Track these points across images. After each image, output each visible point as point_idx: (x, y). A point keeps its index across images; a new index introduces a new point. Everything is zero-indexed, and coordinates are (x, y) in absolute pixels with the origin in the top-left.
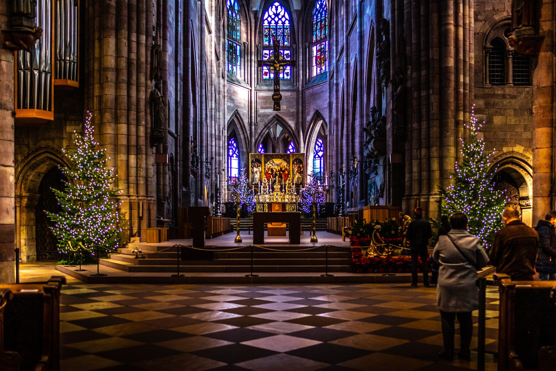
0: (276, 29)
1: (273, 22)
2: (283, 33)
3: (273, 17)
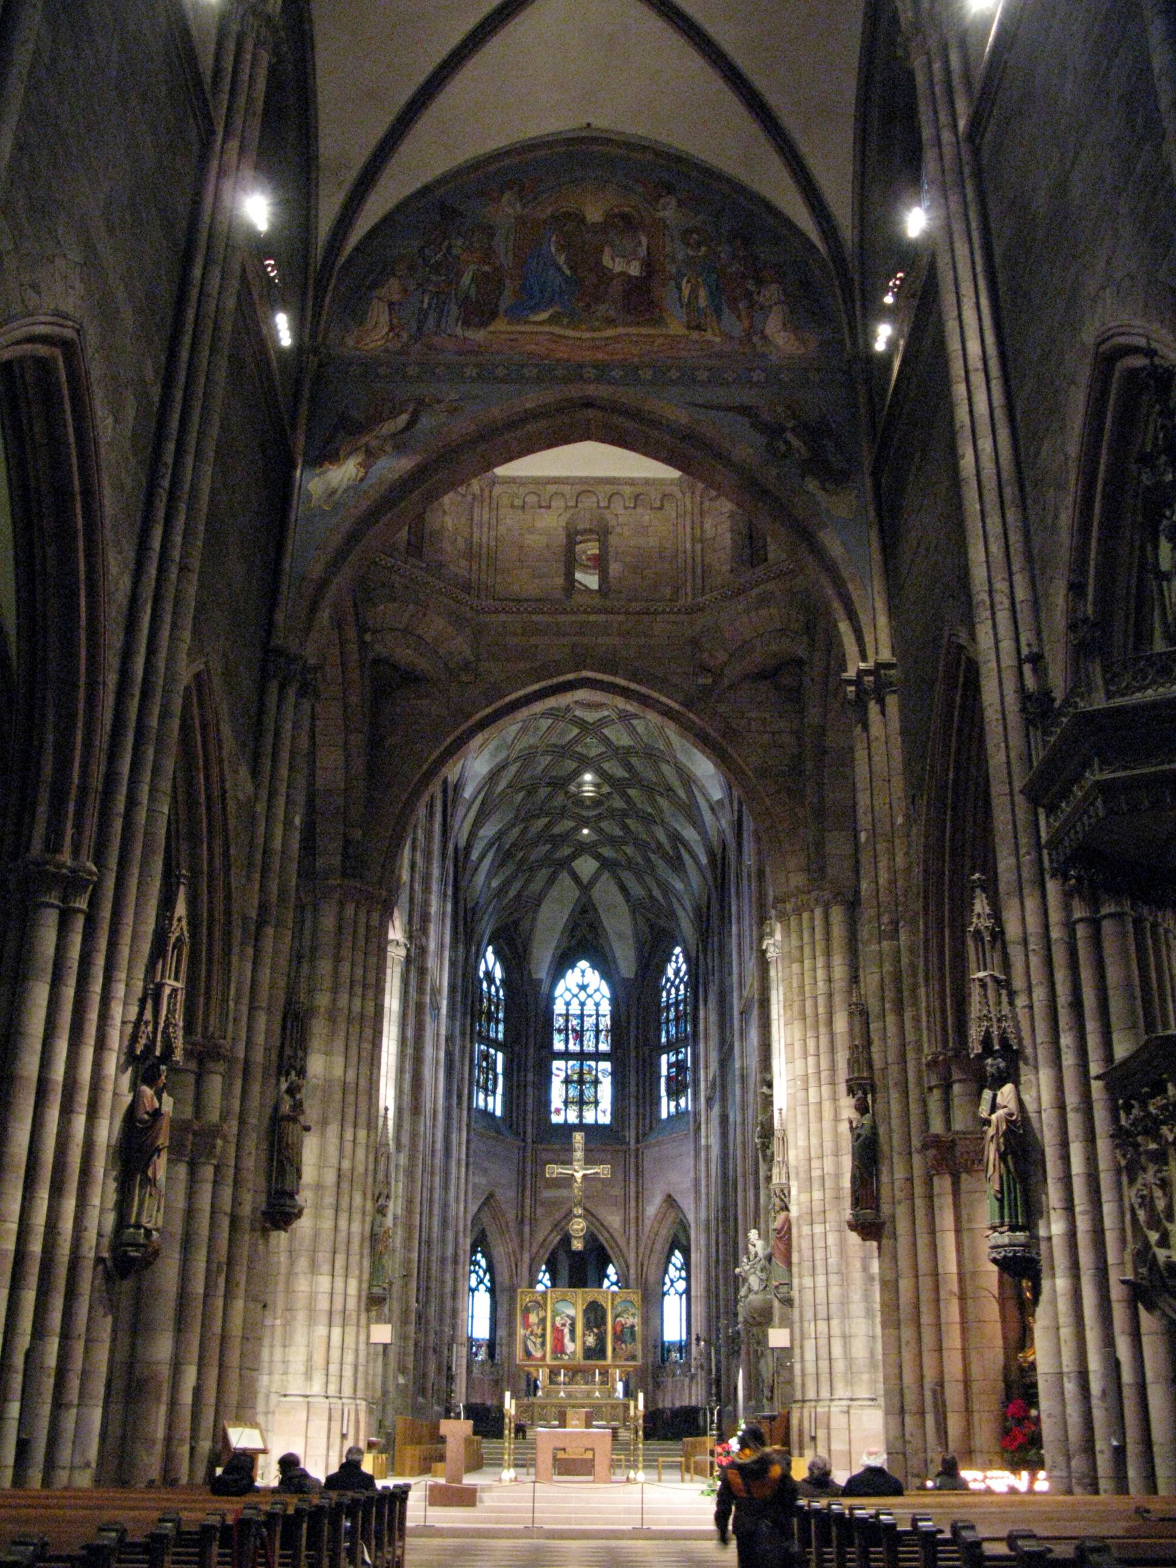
0: (581, 1017)
1: (575, 1002)
2: (597, 1025)
3: (575, 990)
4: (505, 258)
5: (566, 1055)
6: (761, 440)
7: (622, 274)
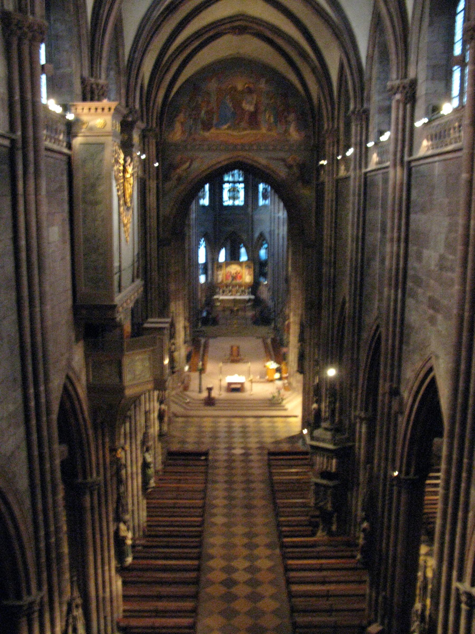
4: (213, 104)
5: (229, 182)
6: (287, 170)
7: (248, 111)
